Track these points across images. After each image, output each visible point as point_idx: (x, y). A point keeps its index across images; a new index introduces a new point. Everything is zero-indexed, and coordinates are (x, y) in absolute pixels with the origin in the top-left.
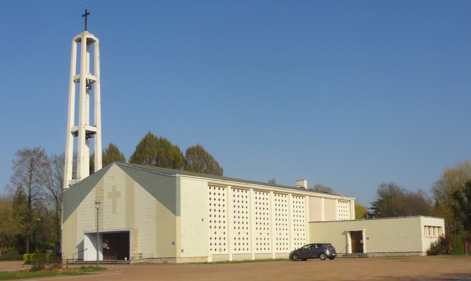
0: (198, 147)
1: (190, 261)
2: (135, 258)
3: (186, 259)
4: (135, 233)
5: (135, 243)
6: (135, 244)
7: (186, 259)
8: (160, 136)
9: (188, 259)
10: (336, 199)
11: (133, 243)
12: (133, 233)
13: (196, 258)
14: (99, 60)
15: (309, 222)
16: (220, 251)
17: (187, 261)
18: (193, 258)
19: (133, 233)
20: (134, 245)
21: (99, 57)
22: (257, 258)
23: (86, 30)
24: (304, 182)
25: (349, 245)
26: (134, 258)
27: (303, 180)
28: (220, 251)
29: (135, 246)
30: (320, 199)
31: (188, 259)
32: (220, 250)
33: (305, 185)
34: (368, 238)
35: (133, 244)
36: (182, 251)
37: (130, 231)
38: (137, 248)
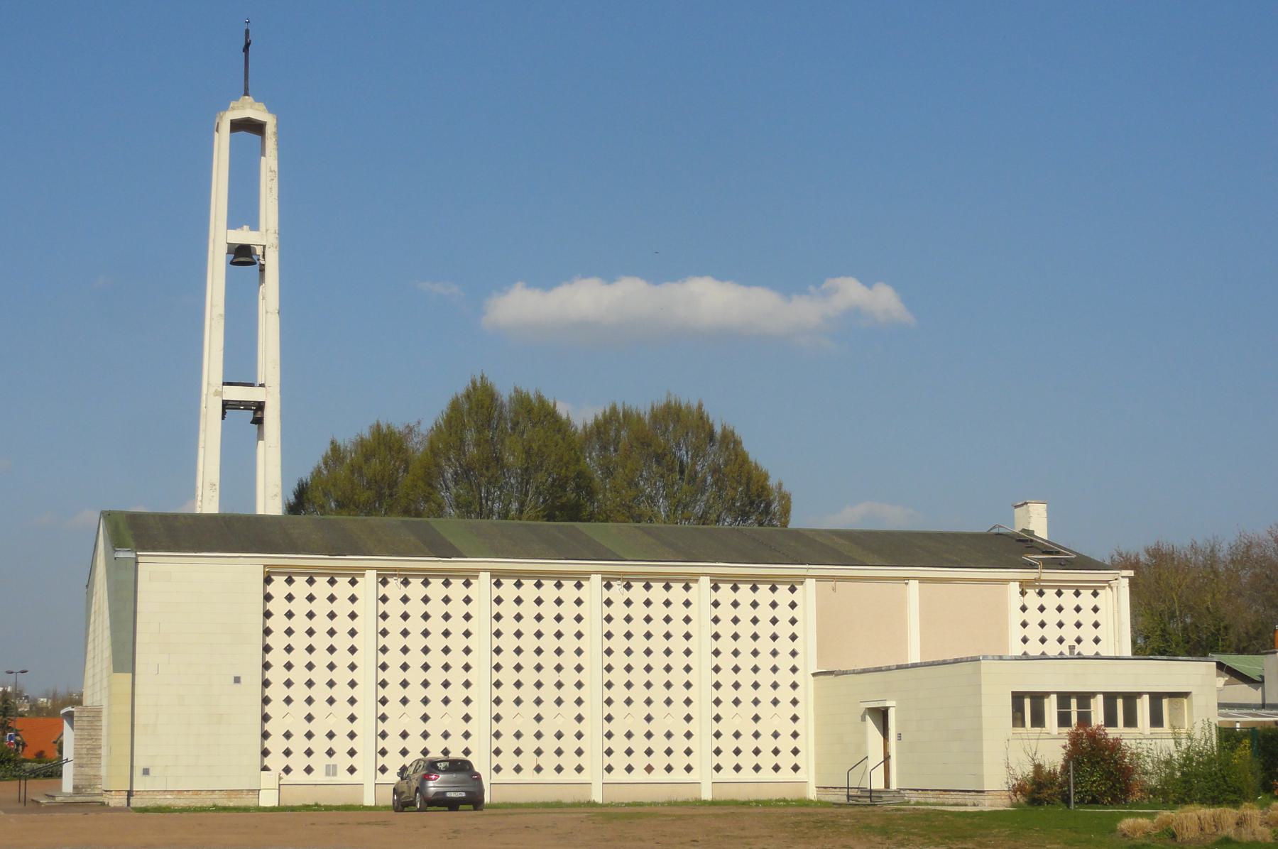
0: (668, 406)
1: (178, 800)
2: (89, 790)
3: (163, 797)
4: (91, 719)
5: (88, 747)
6: (88, 749)
7: (163, 797)
8: (515, 388)
9: (168, 797)
10: (1007, 581)
11: (84, 746)
12: (84, 719)
13: (203, 793)
14: (276, 180)
15: (814, 675)
16: (327, 774)
17: (165, 800)
18: (191, 793)
19: (84, 719)
20: (84, 751)
21: (276, 169)
22: (717, 798)
23: (246, 94)
24: (1028, 511)
25: (892, 757)
26: (82, 788)
27: (1026, 503)
28: (327, 774)
29: (90, 756)
30: (901, 585)
31: (168, 797)
32: (331, 770)
33: (1032, 520)
34: (899, 736)
35: (82, 748)
36: (146, 772)
37: (73, 712)
38: (94, 761)
